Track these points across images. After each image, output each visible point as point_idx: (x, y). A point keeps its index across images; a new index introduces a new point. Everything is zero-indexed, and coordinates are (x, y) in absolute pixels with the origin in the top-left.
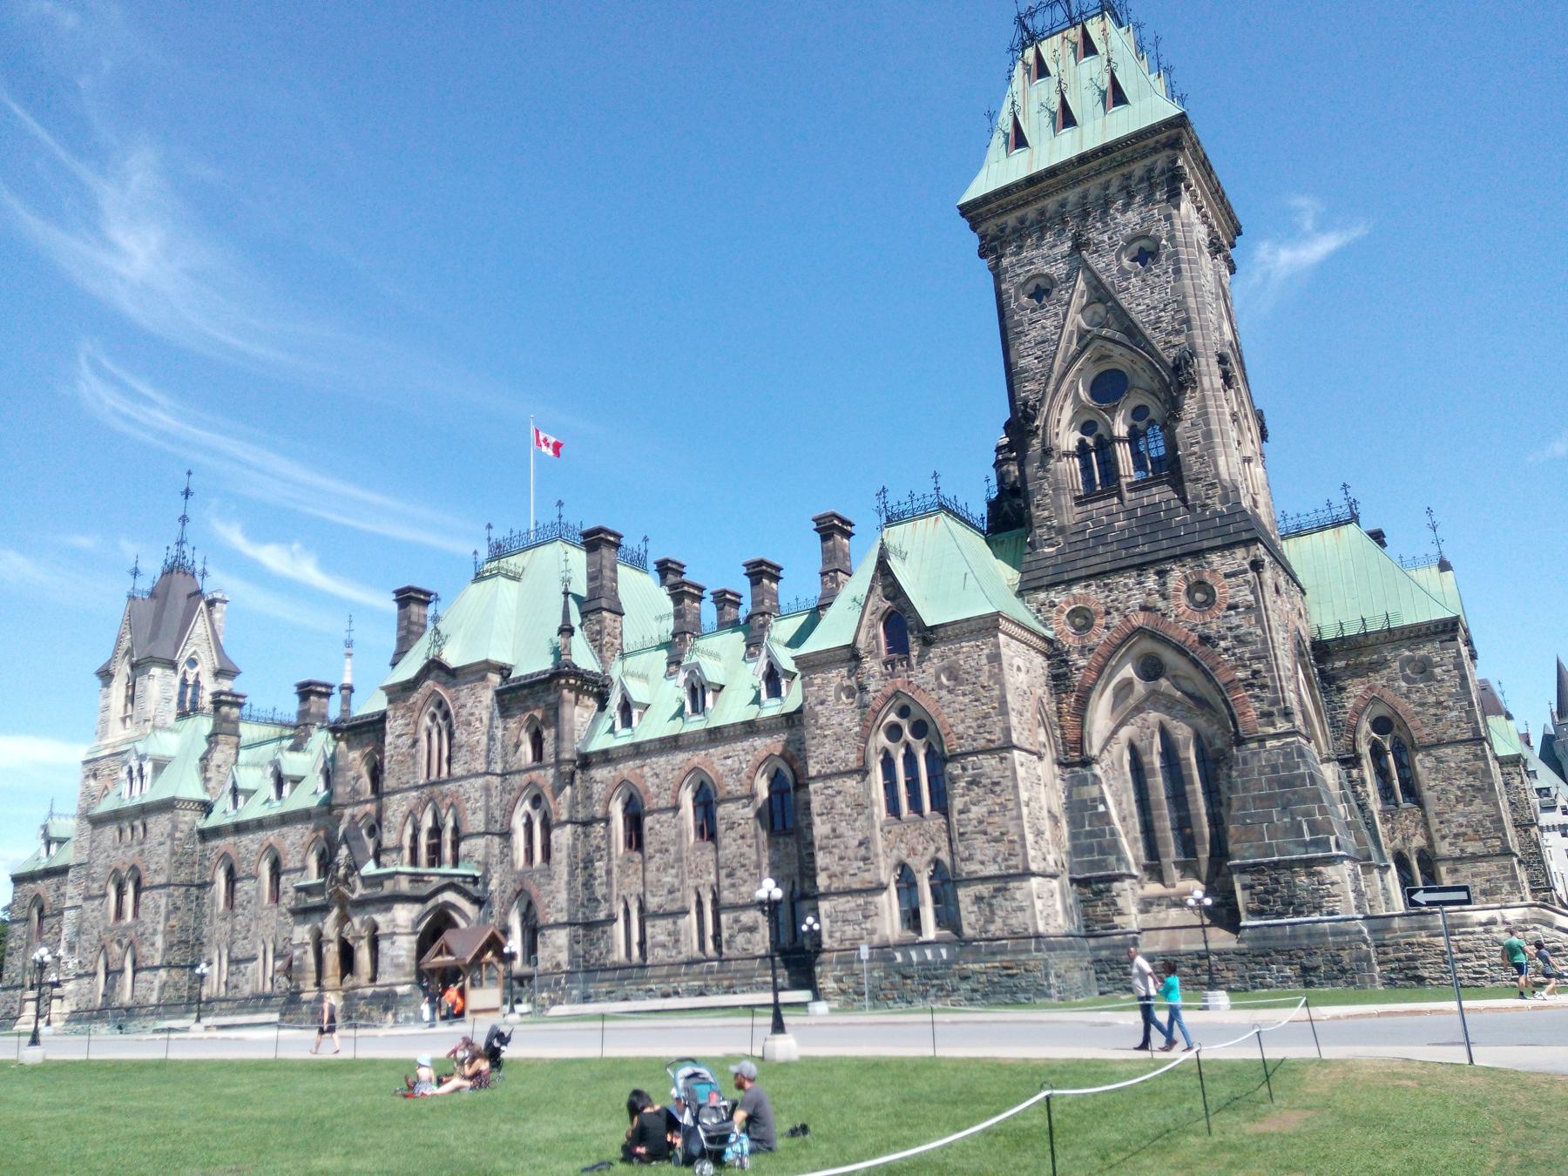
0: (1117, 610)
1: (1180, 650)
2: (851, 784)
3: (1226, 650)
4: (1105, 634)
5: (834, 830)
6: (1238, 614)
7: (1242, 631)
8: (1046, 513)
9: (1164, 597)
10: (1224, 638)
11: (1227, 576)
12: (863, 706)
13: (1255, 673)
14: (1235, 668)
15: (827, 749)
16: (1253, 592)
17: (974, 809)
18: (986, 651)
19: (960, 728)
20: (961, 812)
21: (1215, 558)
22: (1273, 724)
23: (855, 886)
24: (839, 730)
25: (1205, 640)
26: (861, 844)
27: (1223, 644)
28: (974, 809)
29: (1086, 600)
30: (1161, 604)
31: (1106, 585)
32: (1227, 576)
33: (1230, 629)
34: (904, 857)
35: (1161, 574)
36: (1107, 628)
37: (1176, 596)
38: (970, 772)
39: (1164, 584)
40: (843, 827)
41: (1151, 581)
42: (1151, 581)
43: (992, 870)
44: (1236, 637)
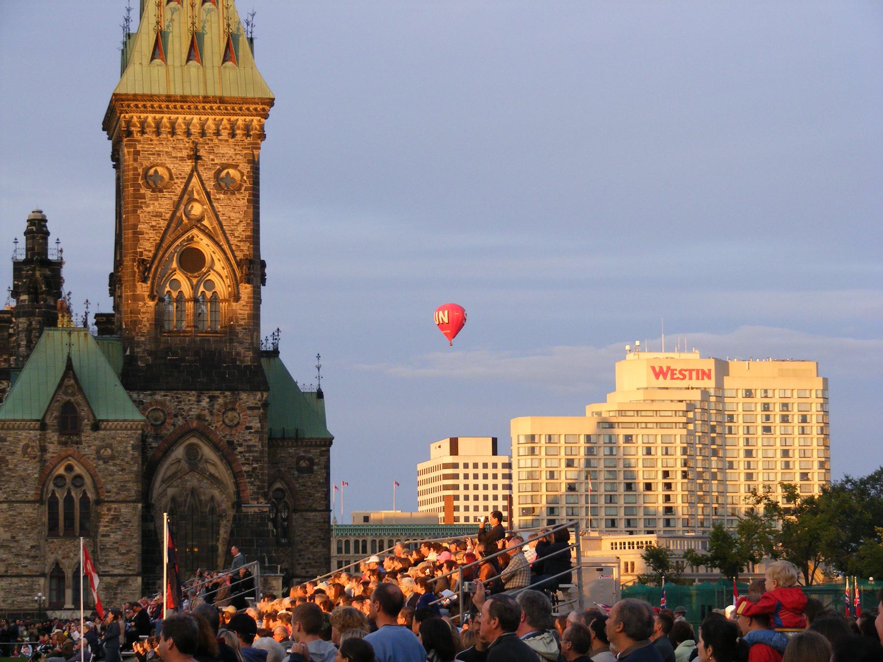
0: (182, 415)
1: (216, 447)
2: (29, 511)
3: (241, 453)
4: (172, 429)
5: (13, 537)
6: (250, 433)
7: (251, 443)
8: (143, 339)
9: (211, 413)
10: (241, 445)
11: (250, 408)
12: (43, 461)
13: (254, 469)
14: (244, 464)
15: (12, 485)
16: (260, 422)
17: (112, 535)
18: (132, 442)
19: (109, 487)
20: (103, 536)
21: (244, 396)
22: (257, 499)
23: (25, 573)
24: (23, 474)
25: (231, 443)
26: (32, 547)
27: (239, 449)
28: (112, 535)
29: (163, 404)
30: (208, 418)
31: (177, 398)
32: (250, 408)
33: (245, 441)
34: (60, 558)
35: (212, 399)
36: (174, 425)
37: (218, 415)
38: (112, 513)
39: (212, 406)
40: (20, 536)
41: (205, 402)
42: (205, 402)
43: (116, 571)
44: (248, 446)
